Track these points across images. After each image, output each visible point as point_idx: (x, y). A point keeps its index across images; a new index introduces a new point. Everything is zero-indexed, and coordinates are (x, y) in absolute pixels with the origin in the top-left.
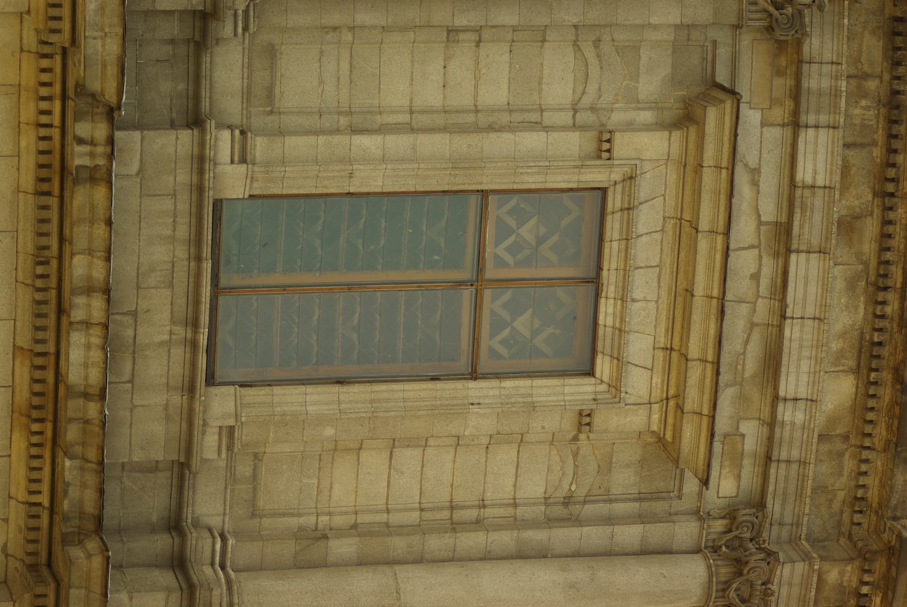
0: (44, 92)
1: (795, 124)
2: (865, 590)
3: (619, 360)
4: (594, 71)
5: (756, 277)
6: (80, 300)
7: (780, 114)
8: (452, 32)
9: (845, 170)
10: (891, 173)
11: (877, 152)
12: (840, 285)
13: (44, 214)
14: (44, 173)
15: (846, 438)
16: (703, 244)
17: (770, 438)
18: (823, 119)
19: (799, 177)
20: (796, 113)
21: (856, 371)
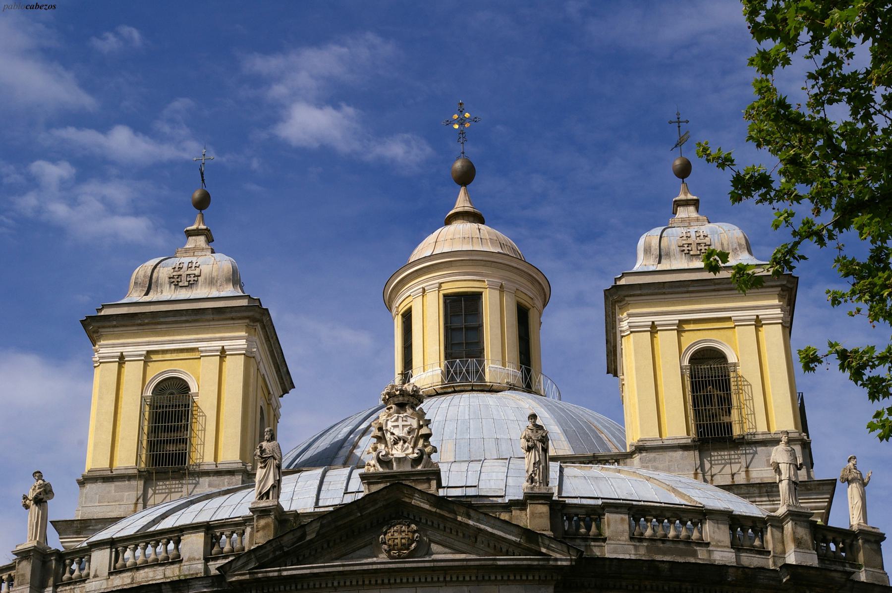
10: (630, 587)
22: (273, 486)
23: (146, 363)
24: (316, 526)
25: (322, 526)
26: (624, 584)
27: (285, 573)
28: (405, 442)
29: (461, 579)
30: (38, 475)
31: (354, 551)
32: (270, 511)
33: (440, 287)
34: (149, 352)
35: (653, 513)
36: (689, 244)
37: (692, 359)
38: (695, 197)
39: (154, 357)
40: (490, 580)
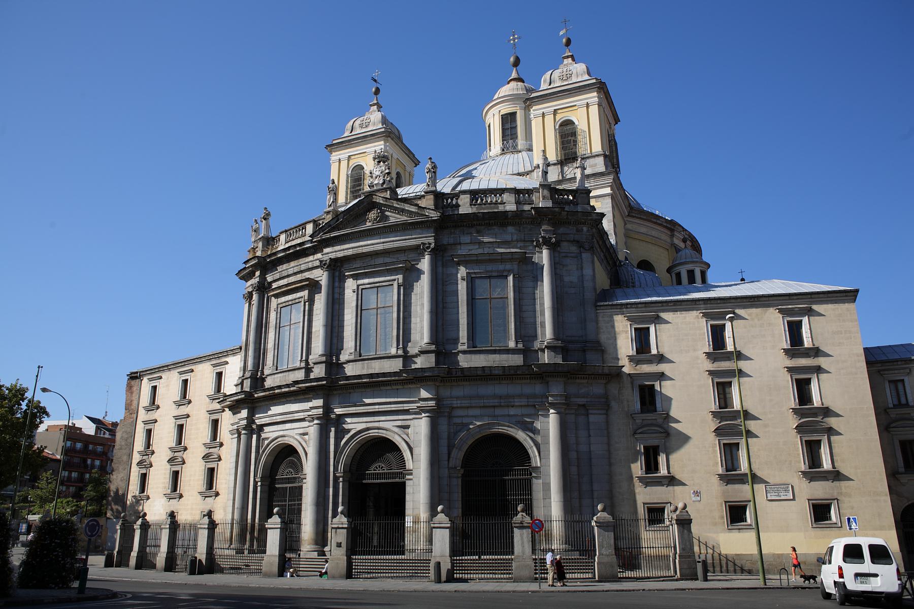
0: (450, 381)
1: (460, 244)
2: (547, 219)
3: (504, 271)
4: (451, 282)
5: (489, 247)
6: (486, 372)
7: (459, 247)
8: (444, 308)
9: (467, 234)
11: (465, 228)
12: (490, 232)
13: (580, 378)
14: (465, 380)
15: (520, 227)
16: (480, 258)
17: (520, 241)
18: (458, 239)
19: (470, 242)
20: (458, 244)
21: (506, 227)
22: (333, 202)
23: (348, 161)
24: (342, 215)
25: (344, 216)
26: (465, 224)
27: (332, 235)
28: (380, 177)
29: (396, 230)
30: (266, 208)
31: (360, 223)
32: (330, 212)
33: (500, 111)
34: (349, 156)
35: (481, 192)
36: (563, 75)
37: (561, 125)
38: (571, 54)
39: (352, 157)
40: (407, 229)
